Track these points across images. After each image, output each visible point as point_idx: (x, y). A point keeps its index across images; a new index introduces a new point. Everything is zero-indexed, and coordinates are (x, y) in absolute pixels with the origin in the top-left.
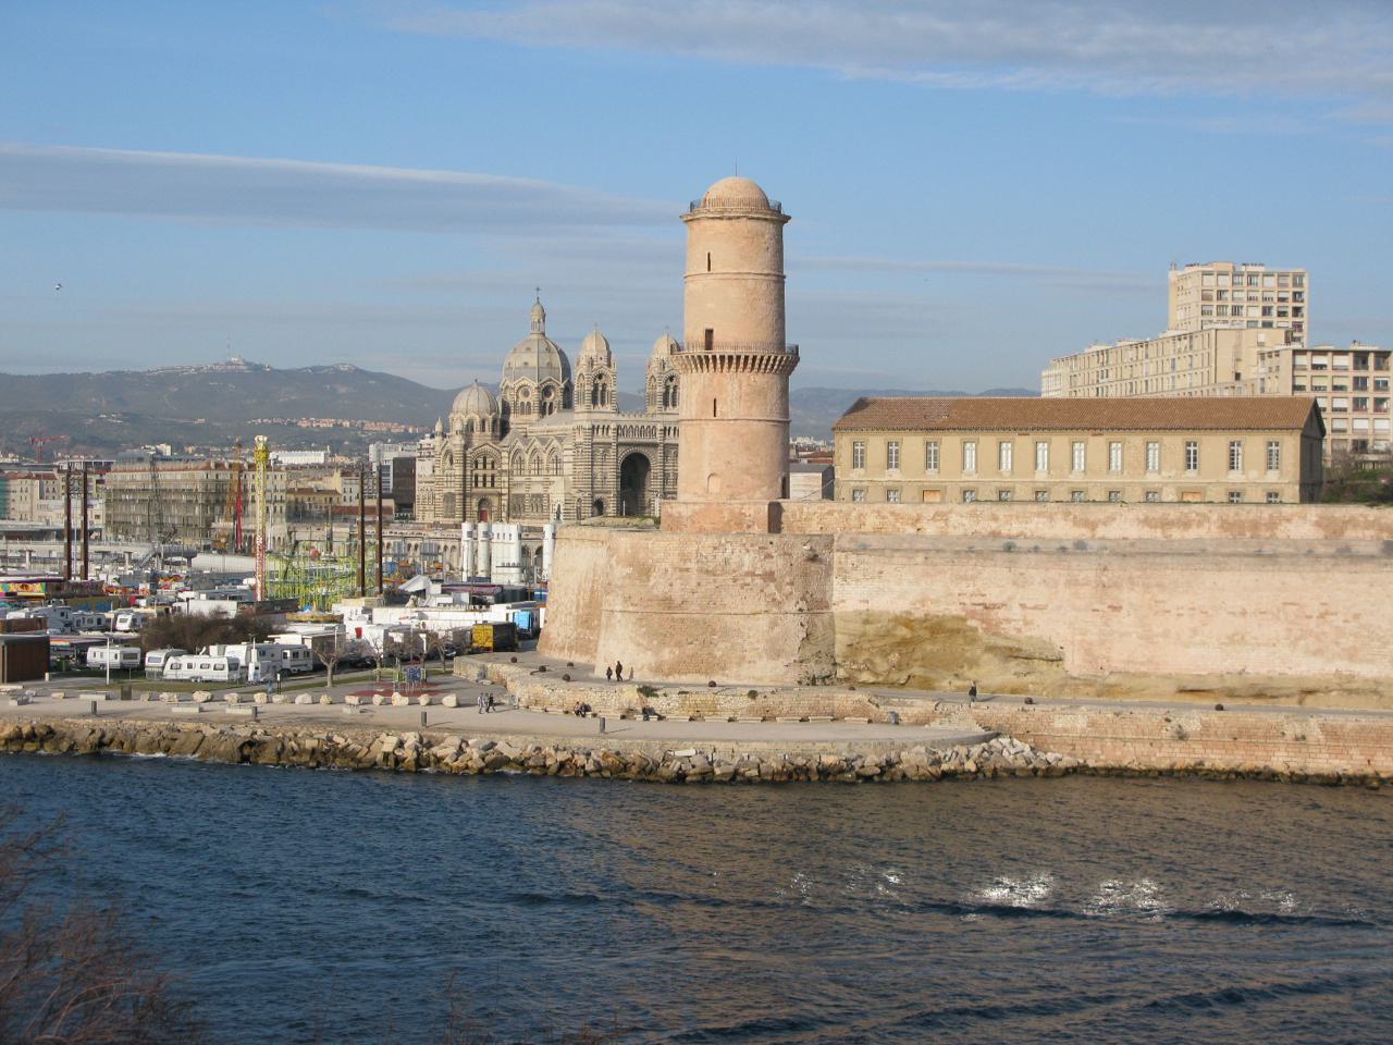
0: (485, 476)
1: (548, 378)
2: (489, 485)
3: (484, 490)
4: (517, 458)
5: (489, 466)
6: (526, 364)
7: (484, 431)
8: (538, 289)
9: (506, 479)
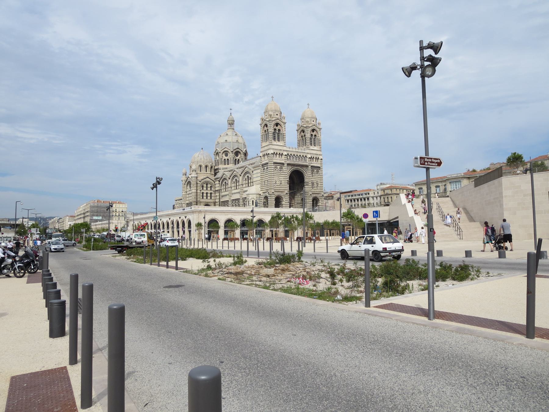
0: (207, 193)
1: (237, 147)
2: (209, 198)
3: (207, 200)
4: (224, 183)
5: (209, 189)
6: (226, 141)
7: (206, 171)
8: (231, 109)
9: (218, 194)
